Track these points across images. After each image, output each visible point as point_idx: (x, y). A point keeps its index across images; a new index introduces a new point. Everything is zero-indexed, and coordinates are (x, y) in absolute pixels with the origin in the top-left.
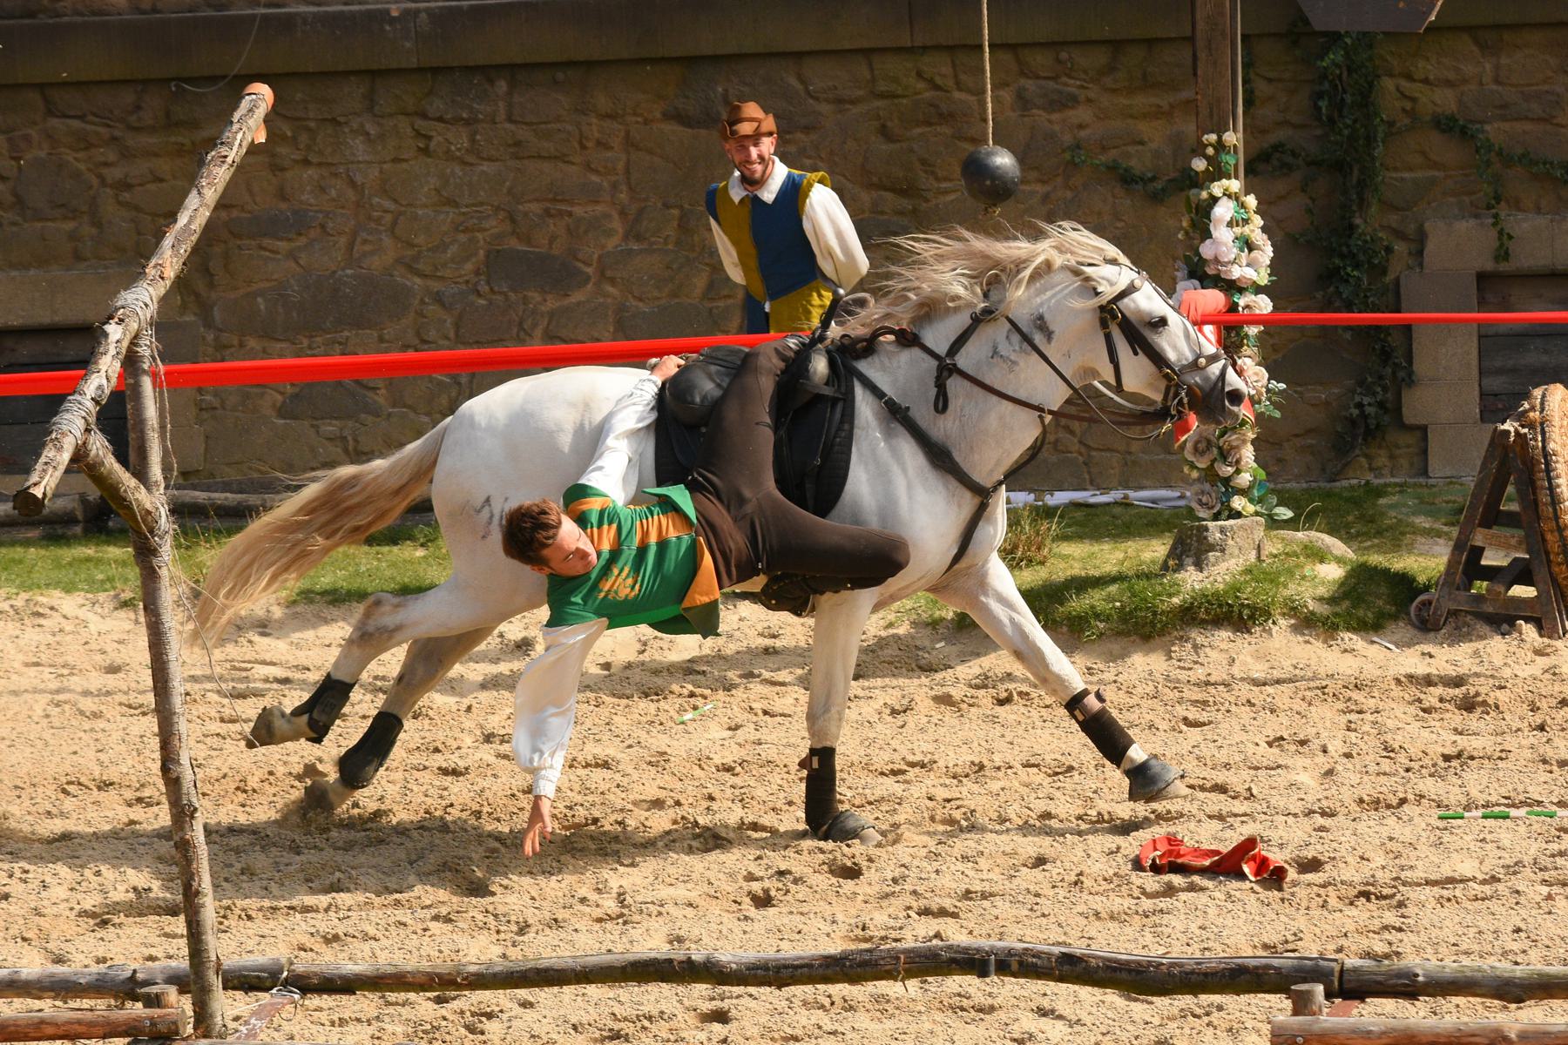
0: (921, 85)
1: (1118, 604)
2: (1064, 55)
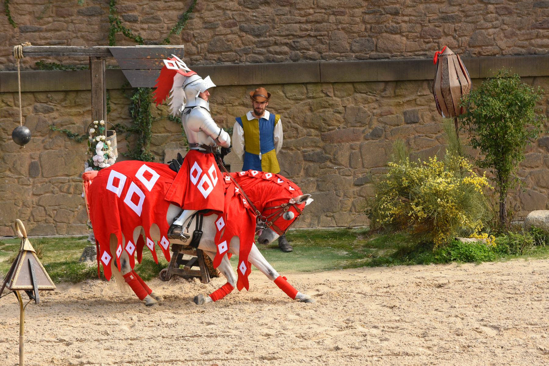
0: (3, 105)
1: (65, 272)
2: (49, 95)
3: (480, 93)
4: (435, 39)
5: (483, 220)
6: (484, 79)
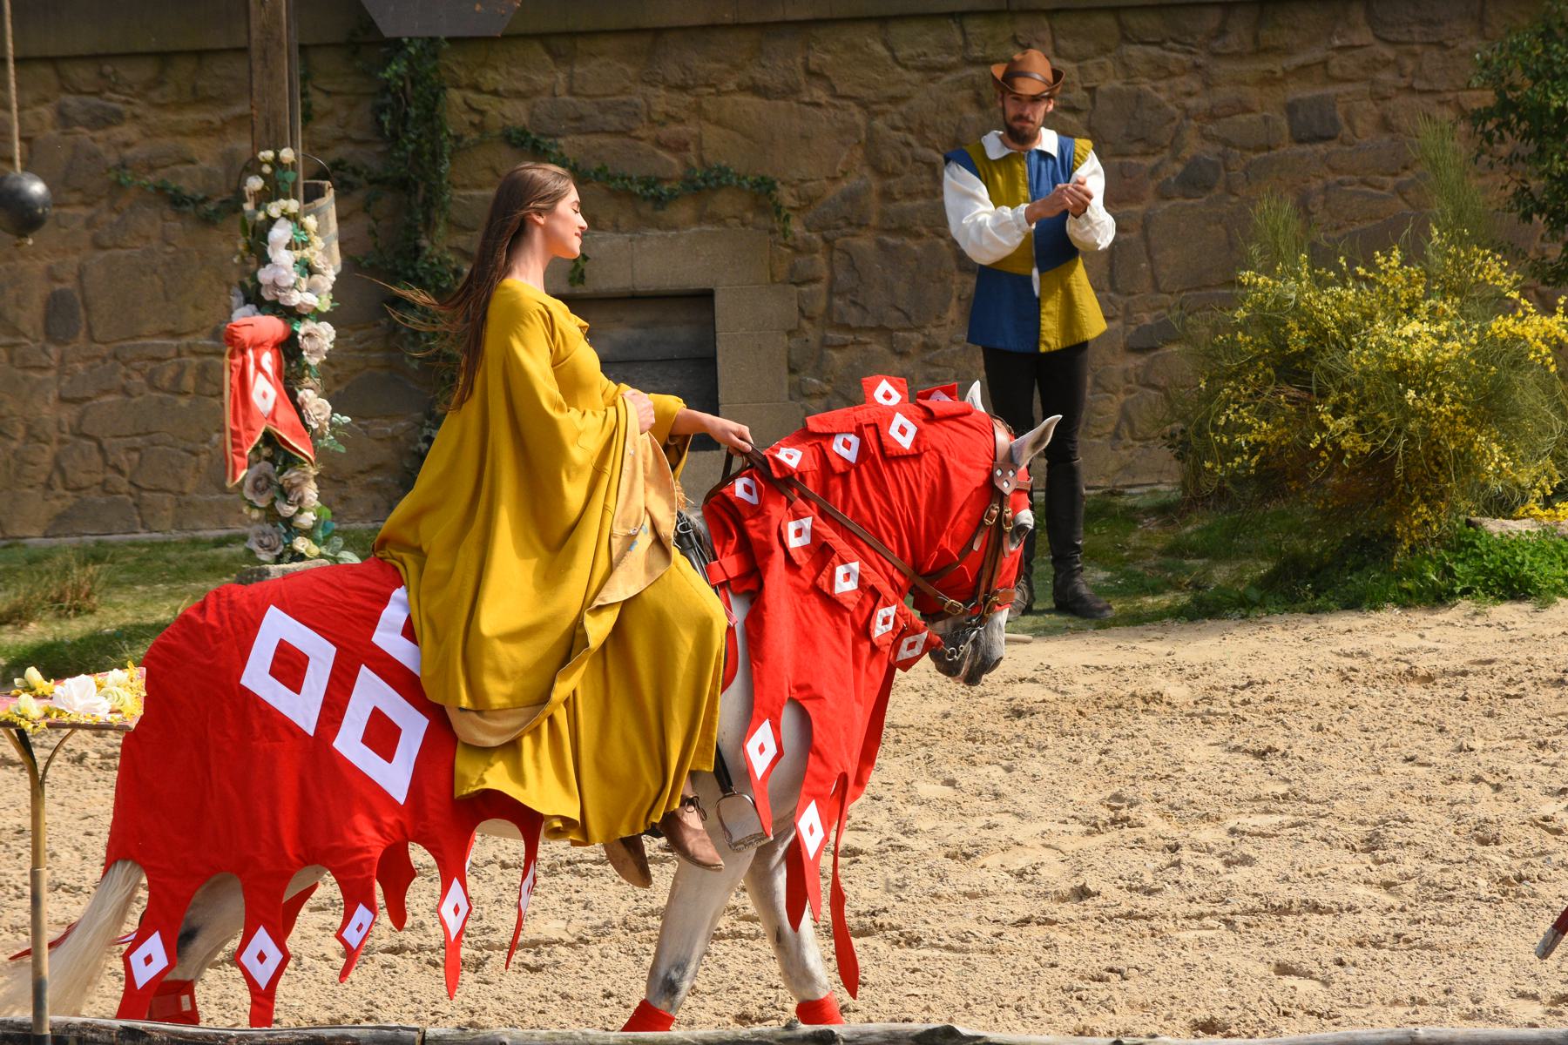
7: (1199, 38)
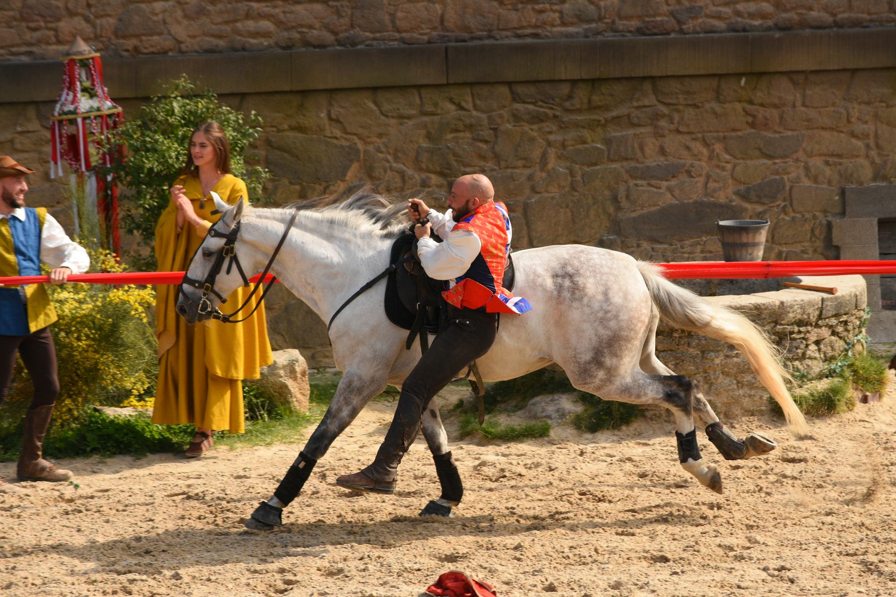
3: (139, 126)
4: (50, 22)
5: (146, 372)
6: (147, 99)
7: (557, 100)
